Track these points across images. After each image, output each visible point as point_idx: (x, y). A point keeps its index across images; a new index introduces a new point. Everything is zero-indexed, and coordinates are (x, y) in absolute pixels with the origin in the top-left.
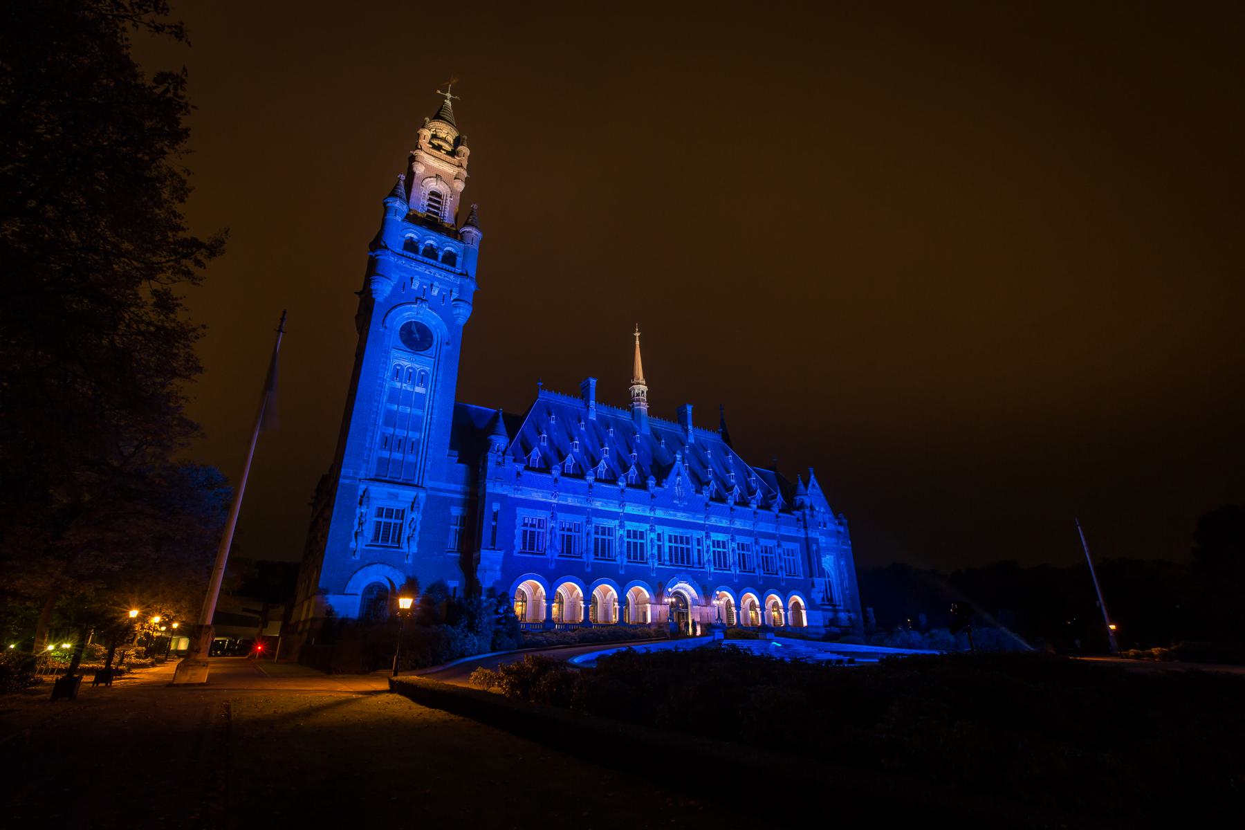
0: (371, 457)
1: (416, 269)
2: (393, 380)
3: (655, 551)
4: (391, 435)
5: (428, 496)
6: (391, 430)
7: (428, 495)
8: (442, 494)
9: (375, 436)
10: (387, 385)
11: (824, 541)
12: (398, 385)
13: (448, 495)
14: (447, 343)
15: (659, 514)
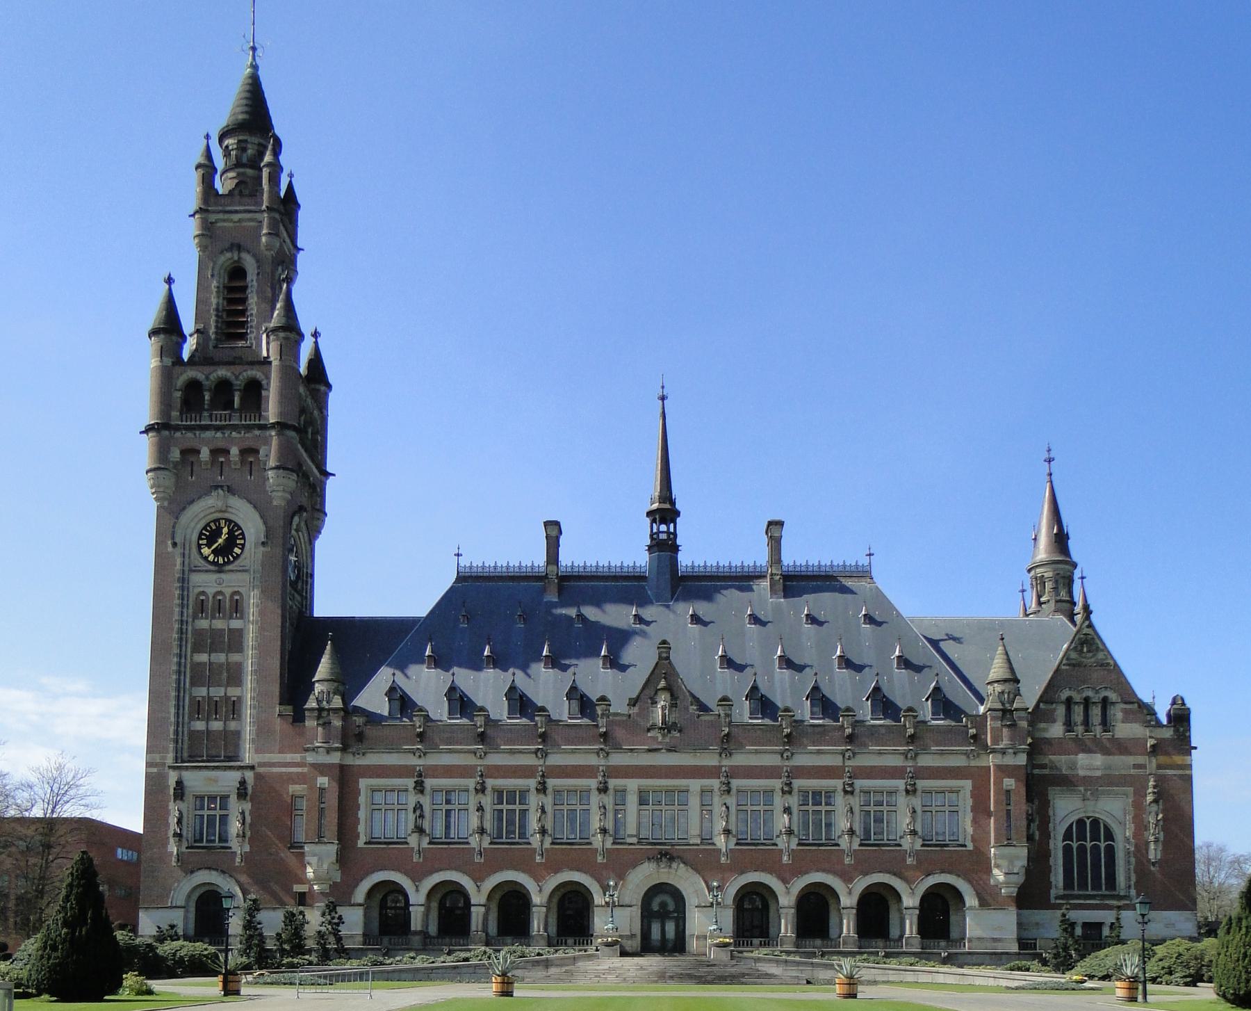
0: (181, 733)
1: (202, 436)
2: (195, 617)
3: (610, 825)
4: (203, 697)
5: (258, 777)
6: (202, 692)
7: (254, 773)
8: (275, 770)
9: (181, 704)
10: (190, 628)
11: (1099, 763)
12: (203, 624)
13: (284, 770)
14: (263, 543)
15: (617, 759)
